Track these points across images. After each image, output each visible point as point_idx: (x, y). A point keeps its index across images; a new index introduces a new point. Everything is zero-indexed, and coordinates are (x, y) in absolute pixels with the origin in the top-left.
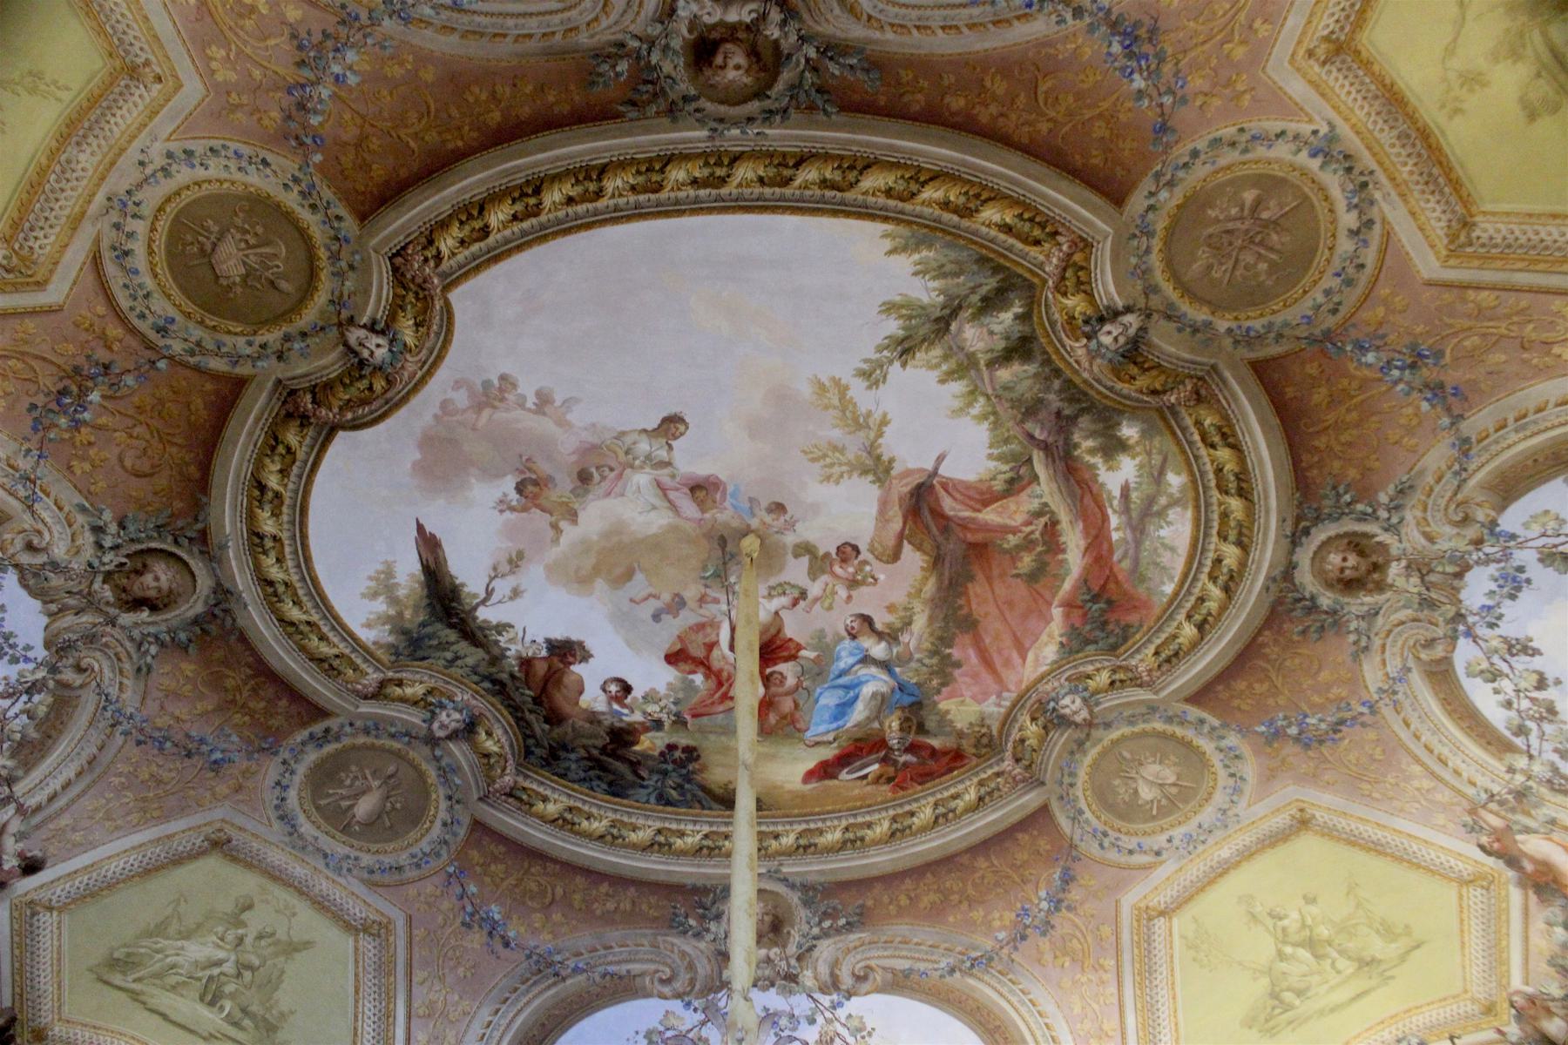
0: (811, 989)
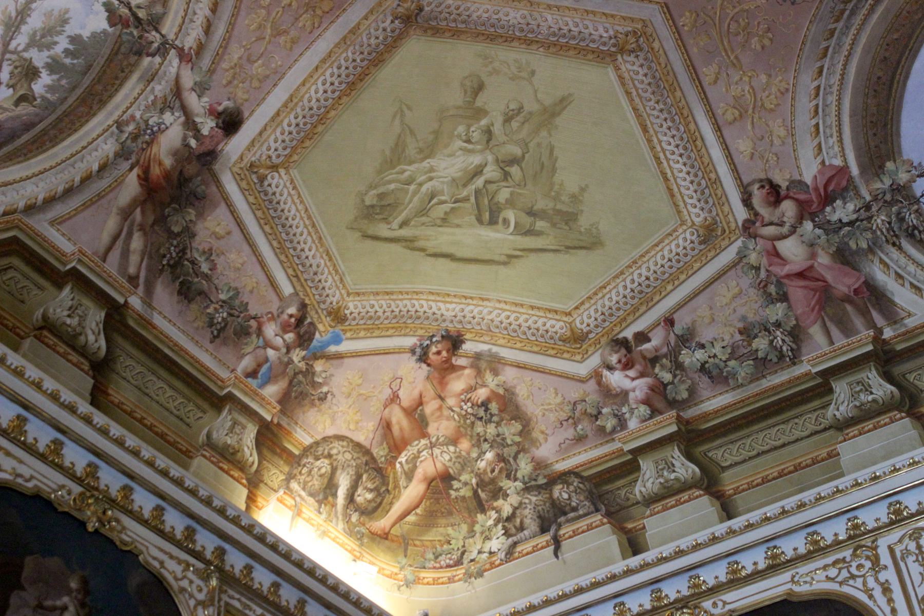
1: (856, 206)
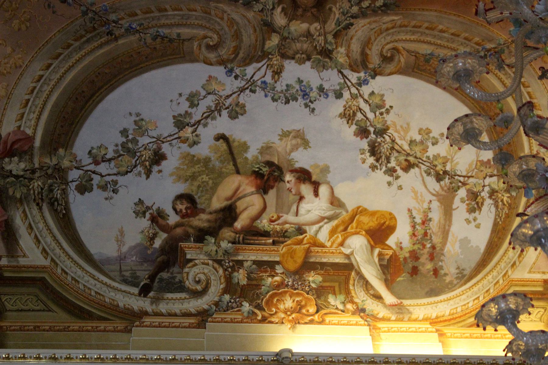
0: (342, 66)
1: (26, 167)
